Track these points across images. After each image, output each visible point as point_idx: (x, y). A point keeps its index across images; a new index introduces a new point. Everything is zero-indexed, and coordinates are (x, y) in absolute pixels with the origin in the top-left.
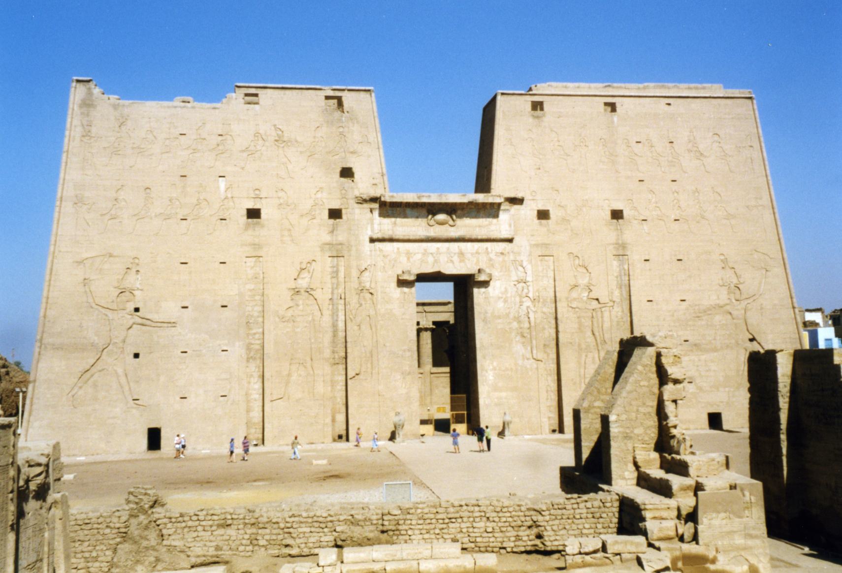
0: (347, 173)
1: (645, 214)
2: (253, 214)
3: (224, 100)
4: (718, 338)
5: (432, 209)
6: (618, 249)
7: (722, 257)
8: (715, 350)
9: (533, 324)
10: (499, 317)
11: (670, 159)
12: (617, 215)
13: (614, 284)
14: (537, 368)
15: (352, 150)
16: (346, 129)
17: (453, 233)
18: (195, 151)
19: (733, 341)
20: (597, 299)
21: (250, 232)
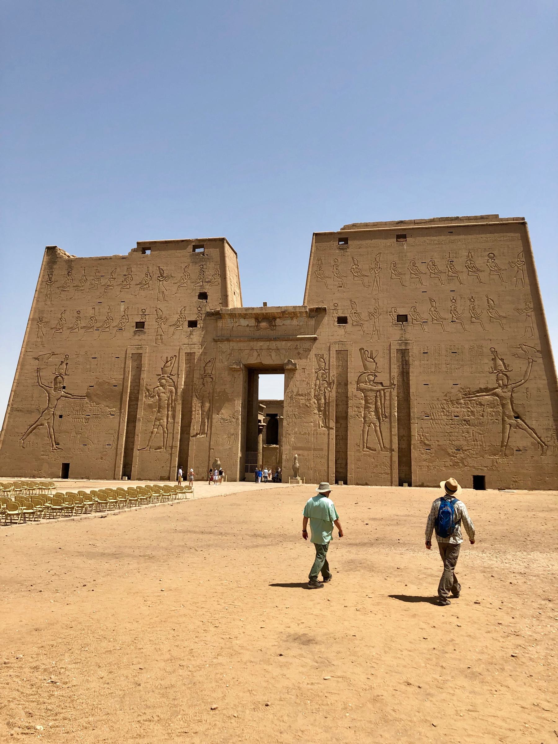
0: (203, 296)
1: (426, 316)
2: (140, 325)
4: (485, 414)
6: (400, 345)
8: (481, 424)
9: (327, 401)
10: (302, 395)
11: (450, 273)
12: (402, 318)
13: (395, 372)
14: (329, 434)
15: (207, 280)
17: (272, 334)
19: (500, 418)
21: (137, 337)
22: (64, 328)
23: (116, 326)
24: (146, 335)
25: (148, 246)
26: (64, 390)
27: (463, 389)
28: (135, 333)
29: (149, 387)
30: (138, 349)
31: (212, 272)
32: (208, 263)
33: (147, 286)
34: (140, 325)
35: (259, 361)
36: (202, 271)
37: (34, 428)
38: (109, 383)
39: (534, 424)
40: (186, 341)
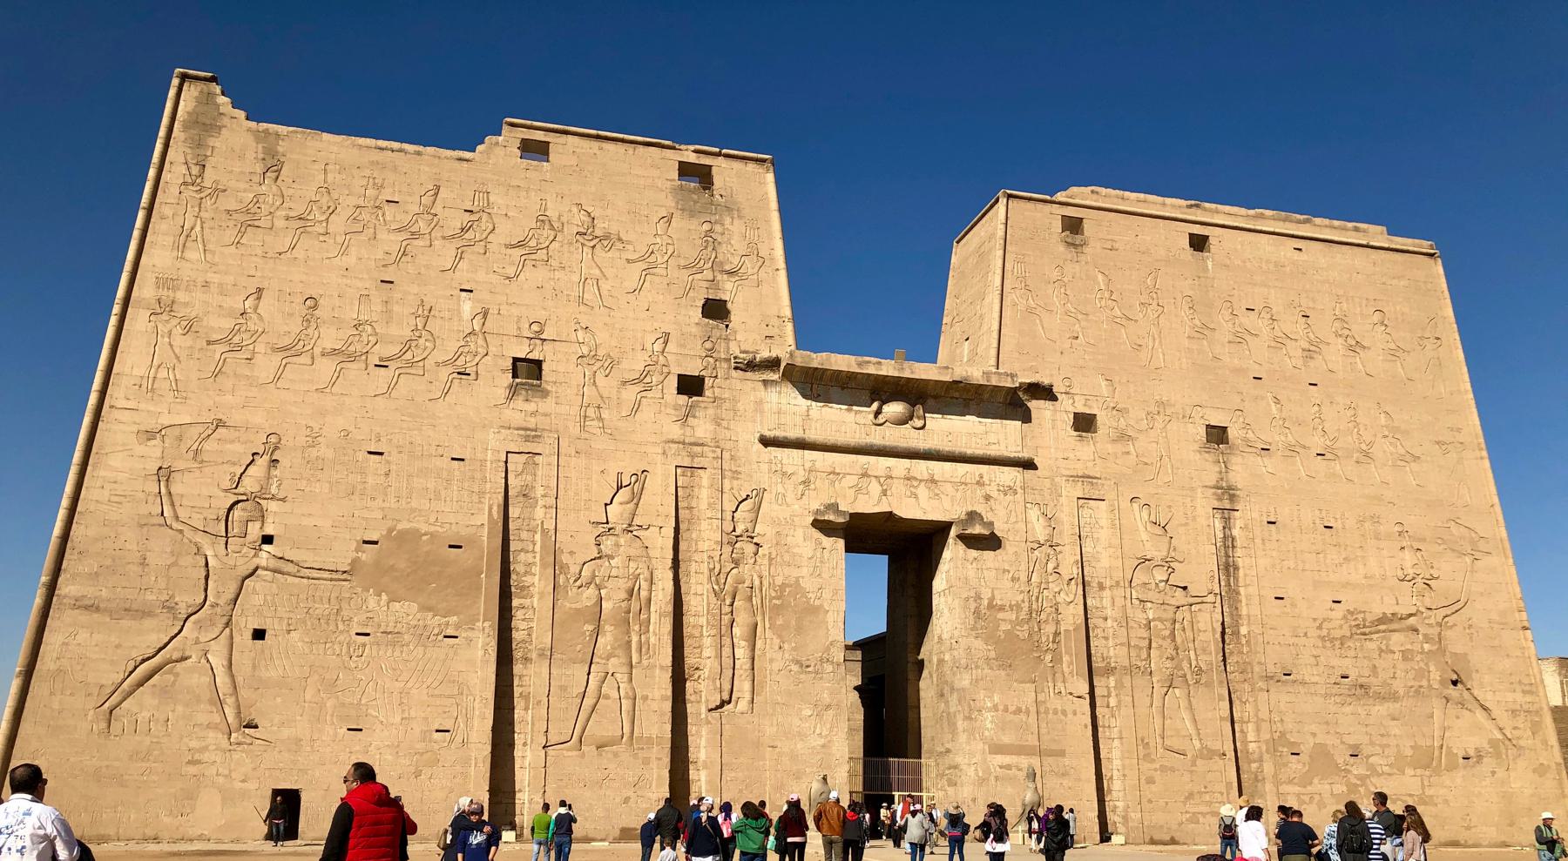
0: (715, 310)
2: (528, 370)
3: (480, 148)
5: (879, 391)
7: (1397, 528)
8: (1394, 697)
10: (1002, 608)
15: (727, 268)
16: (718, 228)
18: (415, 235)
20: (1185, 588)
21: (519, 402)
22: (260, 348)
23: (445, 363)
24: (550, 400)
25: (539, 136)
26: (266, 547)
27: (1352, 613)
28: (513, 391)
29: (565, 558)
30: (527, 439)
31: (738, 245)
32: (728, 220)
33: (542, 254)
34: (528, 370)
35: (883, 508)
36: (711, 240)
37: (149, 671)
38: (432, 534)
39: (1488, 698)
40: (676, 431)
